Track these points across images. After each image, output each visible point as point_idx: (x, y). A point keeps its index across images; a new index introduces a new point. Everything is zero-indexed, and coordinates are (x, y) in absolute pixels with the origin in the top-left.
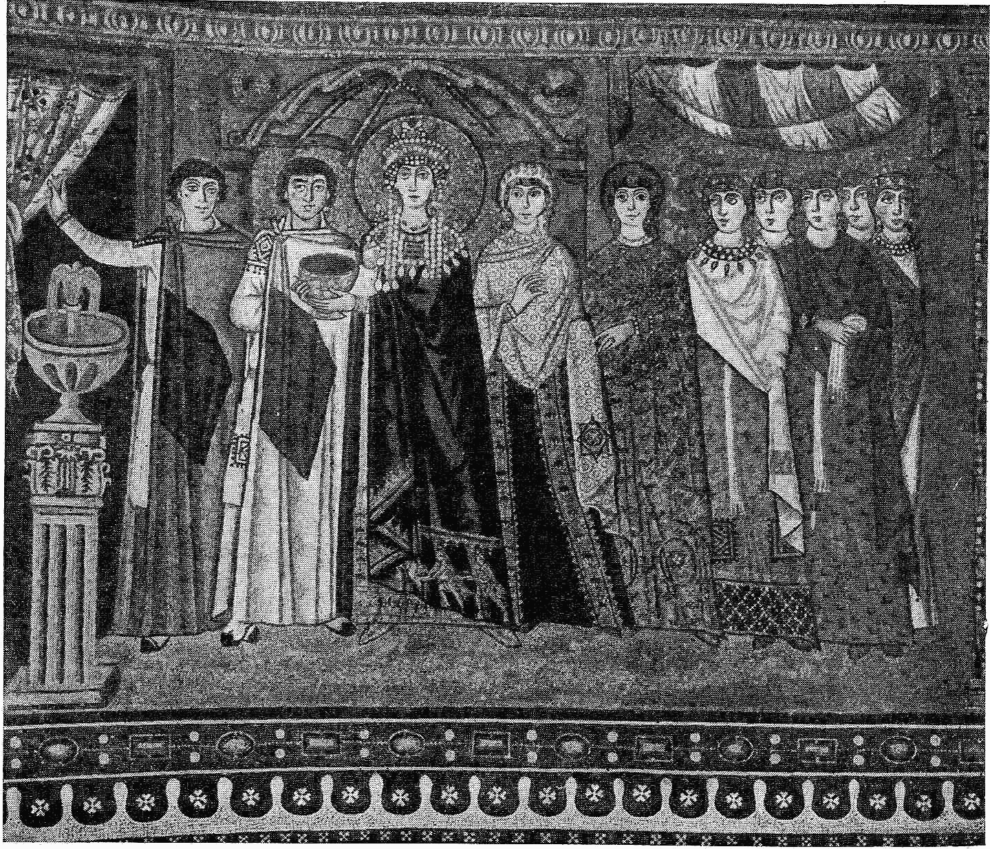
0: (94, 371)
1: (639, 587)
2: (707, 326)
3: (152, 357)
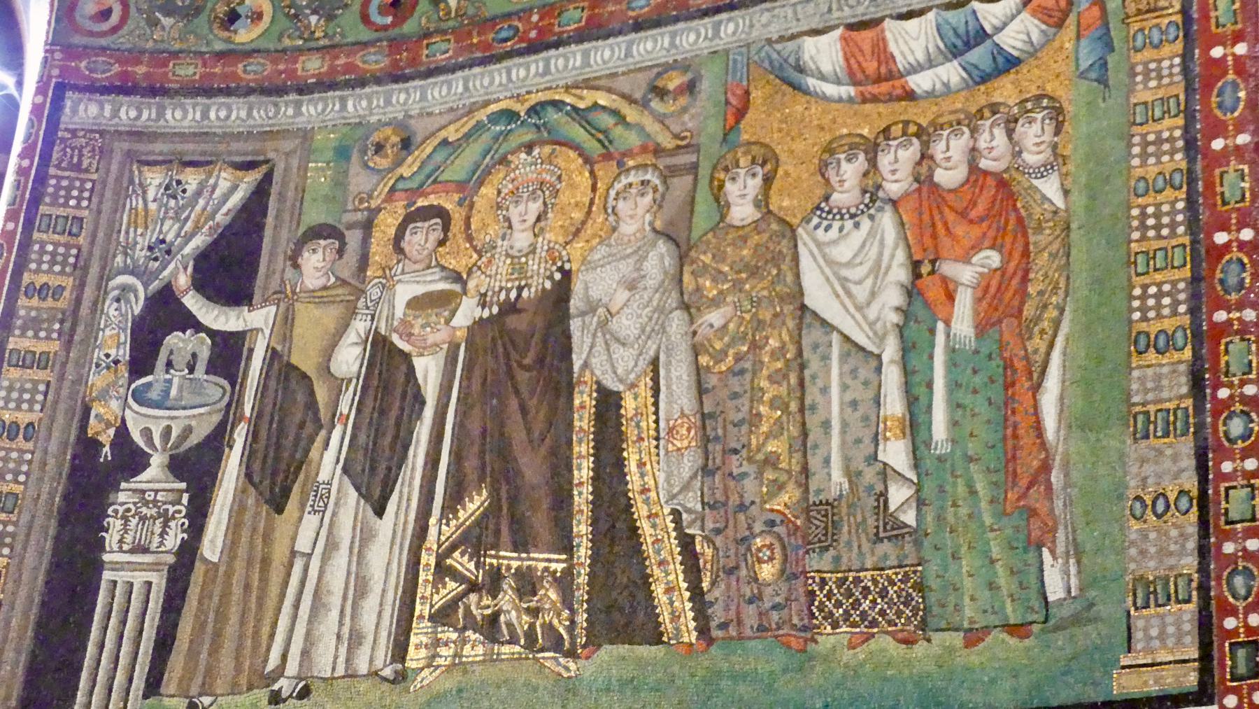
0: (188, 431)
2: (818, 296)
3: (247, 412)
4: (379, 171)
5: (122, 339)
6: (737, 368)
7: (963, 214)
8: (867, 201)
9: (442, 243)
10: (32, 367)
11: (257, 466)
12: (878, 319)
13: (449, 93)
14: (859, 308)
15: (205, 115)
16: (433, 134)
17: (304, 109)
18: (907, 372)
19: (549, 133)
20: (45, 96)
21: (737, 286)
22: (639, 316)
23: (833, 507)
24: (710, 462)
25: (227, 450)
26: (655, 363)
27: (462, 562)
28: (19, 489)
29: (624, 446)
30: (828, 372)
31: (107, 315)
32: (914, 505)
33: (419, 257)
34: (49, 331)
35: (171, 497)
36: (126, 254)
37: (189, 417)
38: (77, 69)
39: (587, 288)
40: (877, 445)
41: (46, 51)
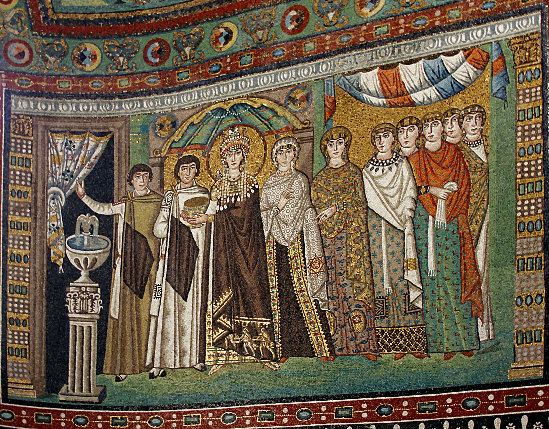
11: (128, 277)
18: (416, 239)
21: (336, 197)
25: (114, 269)
30: (381, 238)
31: (50, 206)
36: (53, 177)
37: (94, 254)
40: (404, 272)
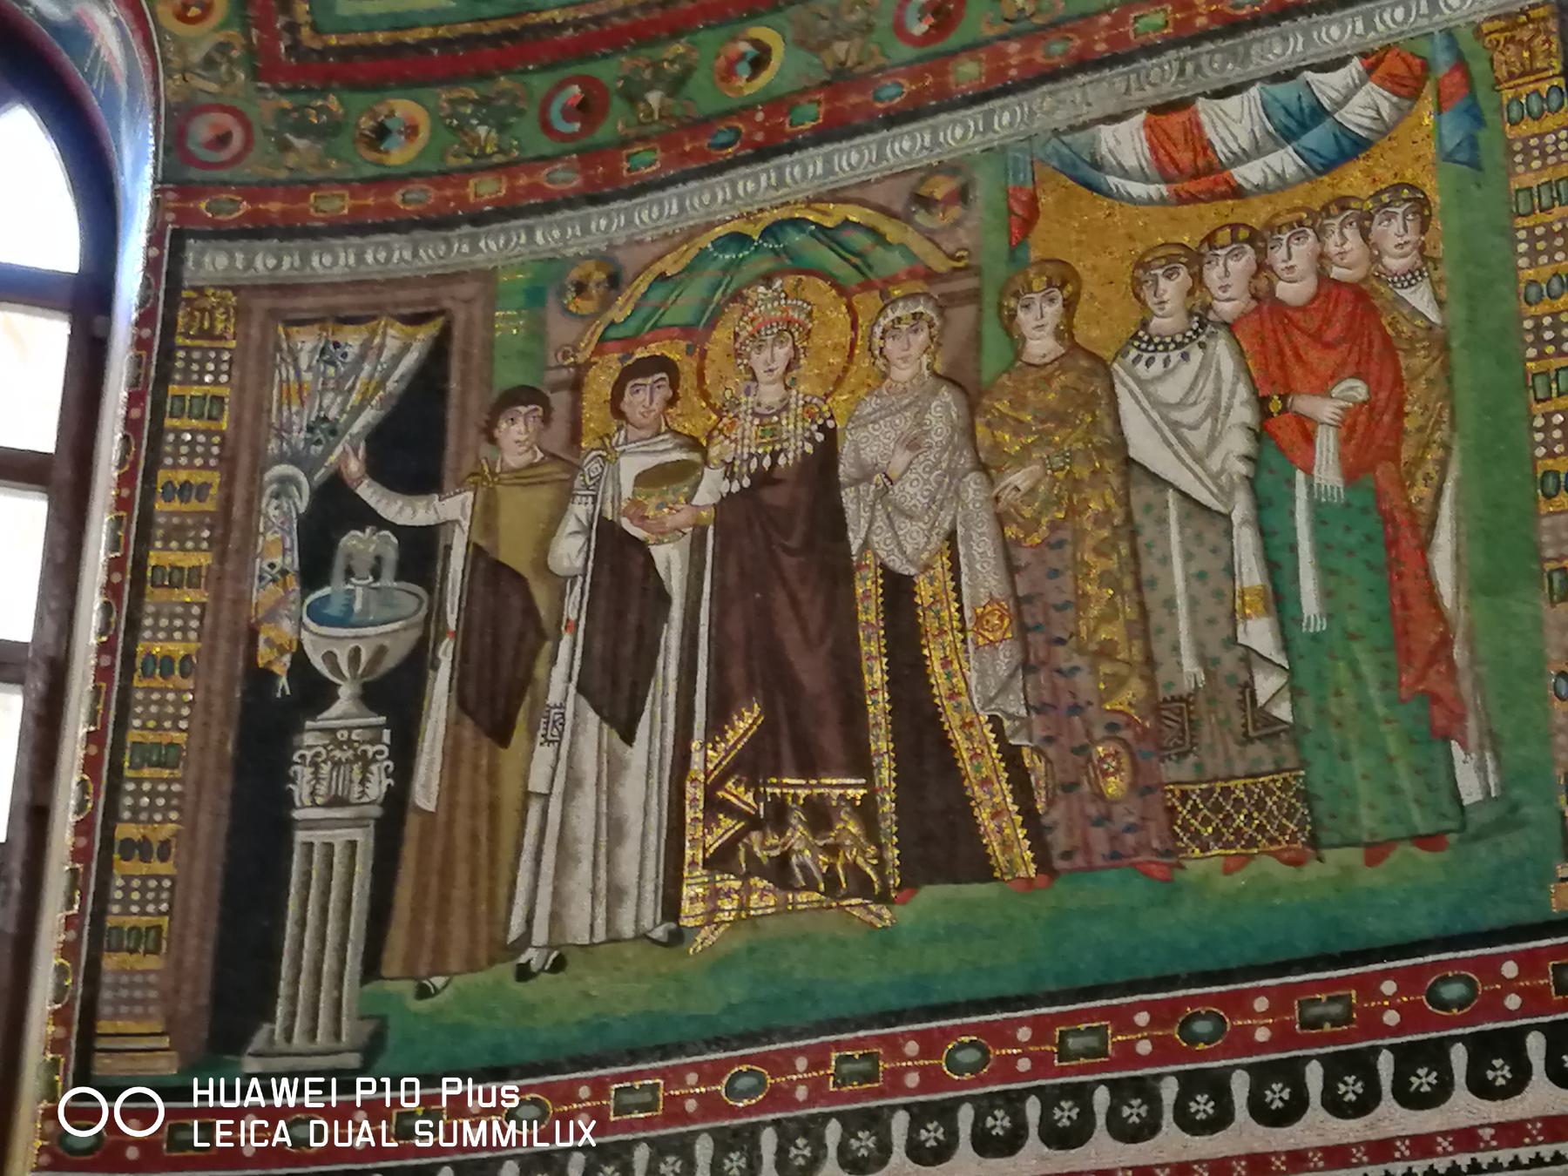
0: (381, 652)
1: (1056, 814)
2: (1145, 444)
3: (452, 625)
4: (583, 317)
5: (288, 545)
6: (1053, 540)
7: (1316, 337)
8: (1195, 326)
9: (671, 402)
10: (179, 586)
11: (471, 690)
12: (1222, 471)
13: (661, 215)
14: (1199, 460)
15: (360, 258)
16: (646, 267)
17: (482, 244)
18: (1263, 533)
19: (792, 259)
20: (160, 246)
21: (1044, 439)
22: (927, 481)
23: (1188, 704)
24: (1032, 657)
25: (431, 672)
26: (951, 536)
27: (737, 793)
28: (178, 737)
29: (924, 642)
30: (1167, 539)
31: (267, 516)
32: (1288, 695)
33: (644, 421)
34: (197, 540)
35: (368, 734)
36: (282, 438)
38: (197, 211)
39: (857, 450)
41: (156, 192)
